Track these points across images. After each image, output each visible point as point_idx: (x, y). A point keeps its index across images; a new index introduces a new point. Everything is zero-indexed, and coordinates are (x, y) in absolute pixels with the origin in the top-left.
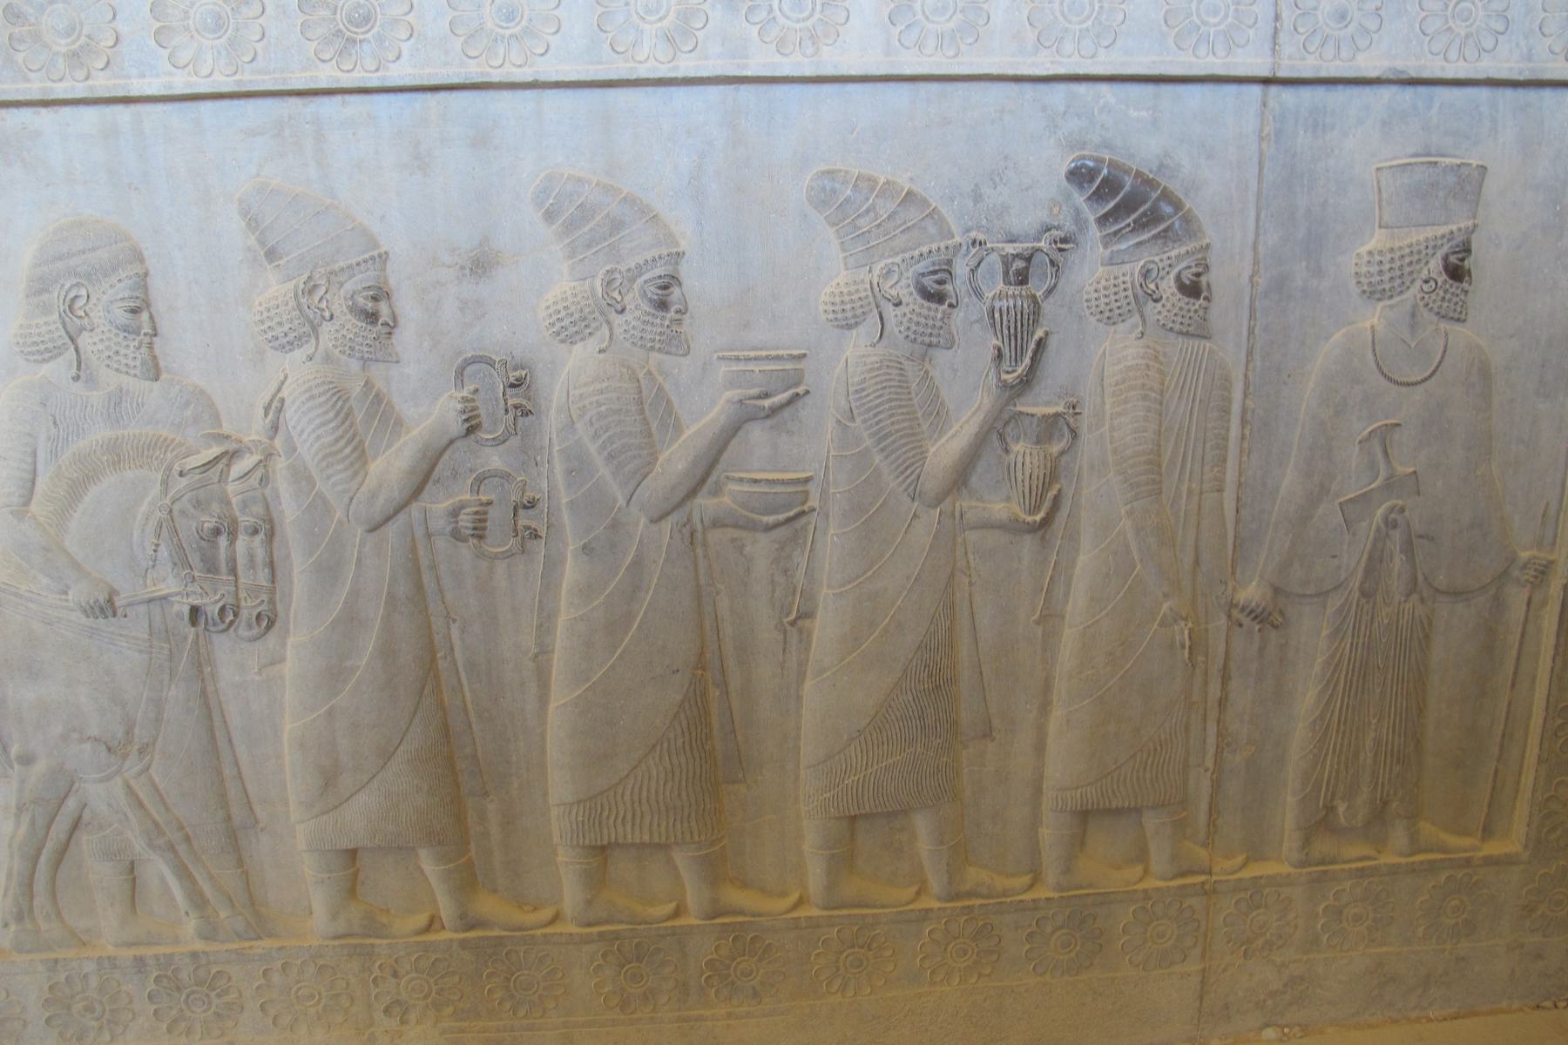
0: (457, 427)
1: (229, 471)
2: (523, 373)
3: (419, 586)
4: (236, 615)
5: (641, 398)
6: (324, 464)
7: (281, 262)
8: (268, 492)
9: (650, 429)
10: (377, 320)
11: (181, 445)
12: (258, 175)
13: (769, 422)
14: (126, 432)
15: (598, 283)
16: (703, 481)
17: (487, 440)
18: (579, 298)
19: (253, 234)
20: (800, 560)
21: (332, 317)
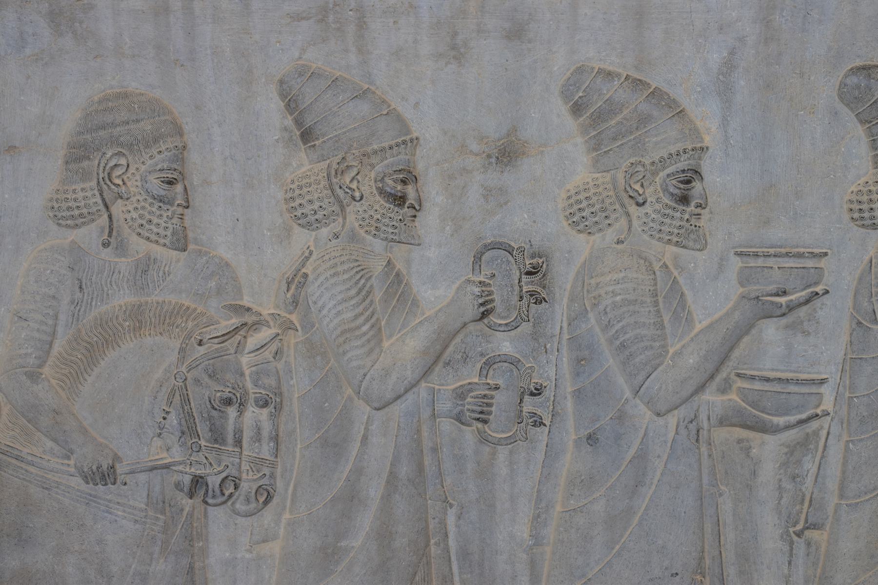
0: (472, 310)
1: (246, 342)
2: (540, 261)
3: (420, 469)
4: (236, 487)
5: (656, 290)
6: (341, 340)
7: (316, 142)
8: (280, 365)
9: (662, 321)
10: (404, 202)
11: (202, 314)
12: (300, 58)
13: (784, 321)
14: (149, 299)
15: (620, 176)
16: (712, 377)
17: (500, 325)
18: (601, 189)
19: (291, 114)
20: (810, 466)
21: (361, 198)
